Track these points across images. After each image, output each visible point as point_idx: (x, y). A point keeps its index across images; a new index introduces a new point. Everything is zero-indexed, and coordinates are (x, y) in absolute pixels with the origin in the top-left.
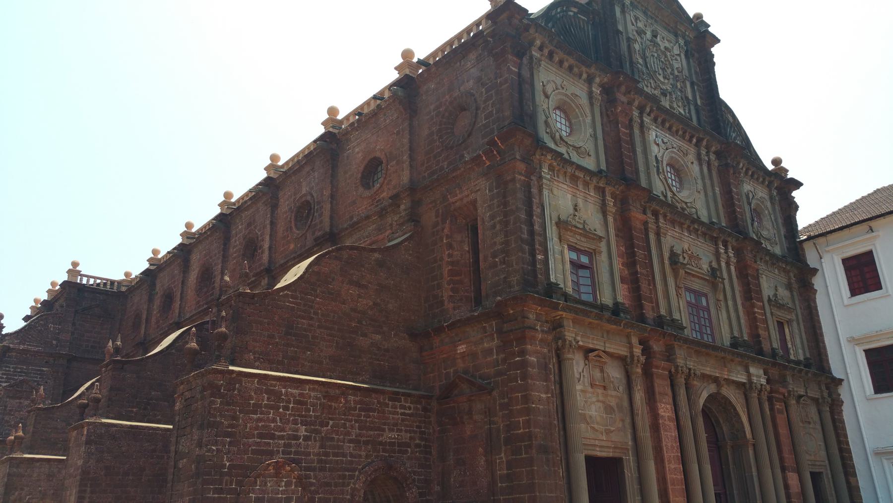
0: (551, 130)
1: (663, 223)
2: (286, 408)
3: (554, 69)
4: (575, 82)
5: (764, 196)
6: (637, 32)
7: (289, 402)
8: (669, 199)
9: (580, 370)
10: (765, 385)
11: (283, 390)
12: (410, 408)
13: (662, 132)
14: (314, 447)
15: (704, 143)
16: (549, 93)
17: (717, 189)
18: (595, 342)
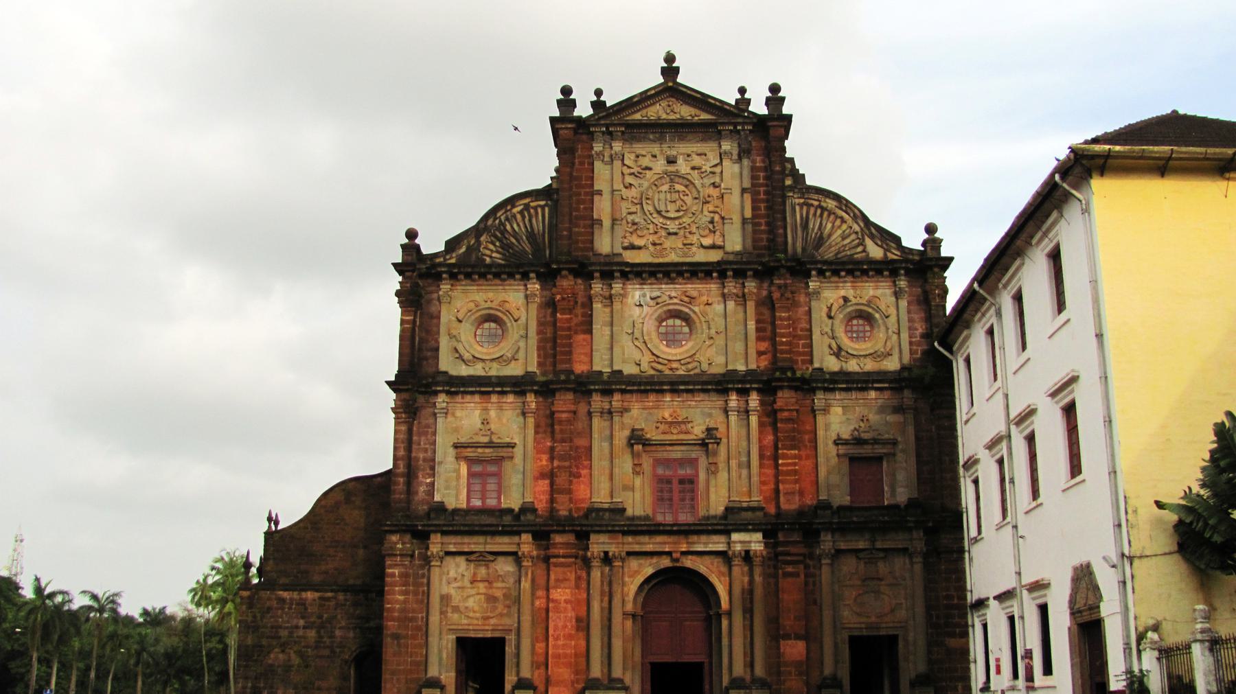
0: (460, 355)
1: (618, 401)
3: (475, 288)
4: (507, 287)
5: (879, 292)
6: (632, 174)
10: (756, 551)
13: (654, 286)
14: (312, 634)
15: (730, 273)
16: (460, 319)
17: (752, 325)
18: (473, 546)
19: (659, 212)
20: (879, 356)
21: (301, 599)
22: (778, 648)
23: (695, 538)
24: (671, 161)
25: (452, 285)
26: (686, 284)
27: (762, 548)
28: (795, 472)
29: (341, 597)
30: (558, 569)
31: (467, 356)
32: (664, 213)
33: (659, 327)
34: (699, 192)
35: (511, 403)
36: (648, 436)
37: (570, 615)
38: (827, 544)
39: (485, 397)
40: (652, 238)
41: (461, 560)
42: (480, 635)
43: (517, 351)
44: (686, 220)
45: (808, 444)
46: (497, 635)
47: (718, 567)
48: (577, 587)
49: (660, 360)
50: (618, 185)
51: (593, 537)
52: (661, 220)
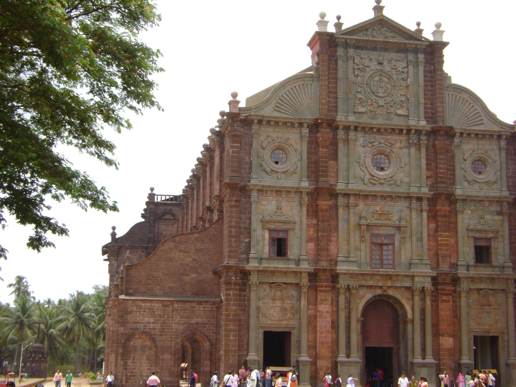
1: (353, 200)
2: (144, 311)
3: (272, 129)
4: (290, 131)
6: (358, 69)
7: (146, 309)
8: (366, 181)
9: (266, 293)
11: (143, 305)
12: (208, 308)
13: (372, 136)
15: (413, 131)
16: (264, 147)
17: (424, 161)
18: (274, 279)
19: (373, 93)
20: (491, 183)
21: (151, 306)
22: (438, 340)
23: (395, 278)
24: (380, 64)
25: (259, 127)
26: (389, 135)
27: (431, 286)
28: (447, 245)
29: (176, 305)
30: (322, 294)
31: (268, 169)
32: (376, 94)
33: (373, 158)
34: (395, 82)
35: (293, 198)
36: (368, 221)
37: (328, 320)
38: (465, 285)
39: (279, 193)
40: (370, 108)
41: (267, 287)
42: (277, 330)
43: (296, 169)
44: (389, 99)
45: (453, 230)
46: (286, 330)
47: (406, 295)
48: (332, 304)
49: (375, 178)
50: (351, 76)
51: (341, 277)
52: (375, 98)
